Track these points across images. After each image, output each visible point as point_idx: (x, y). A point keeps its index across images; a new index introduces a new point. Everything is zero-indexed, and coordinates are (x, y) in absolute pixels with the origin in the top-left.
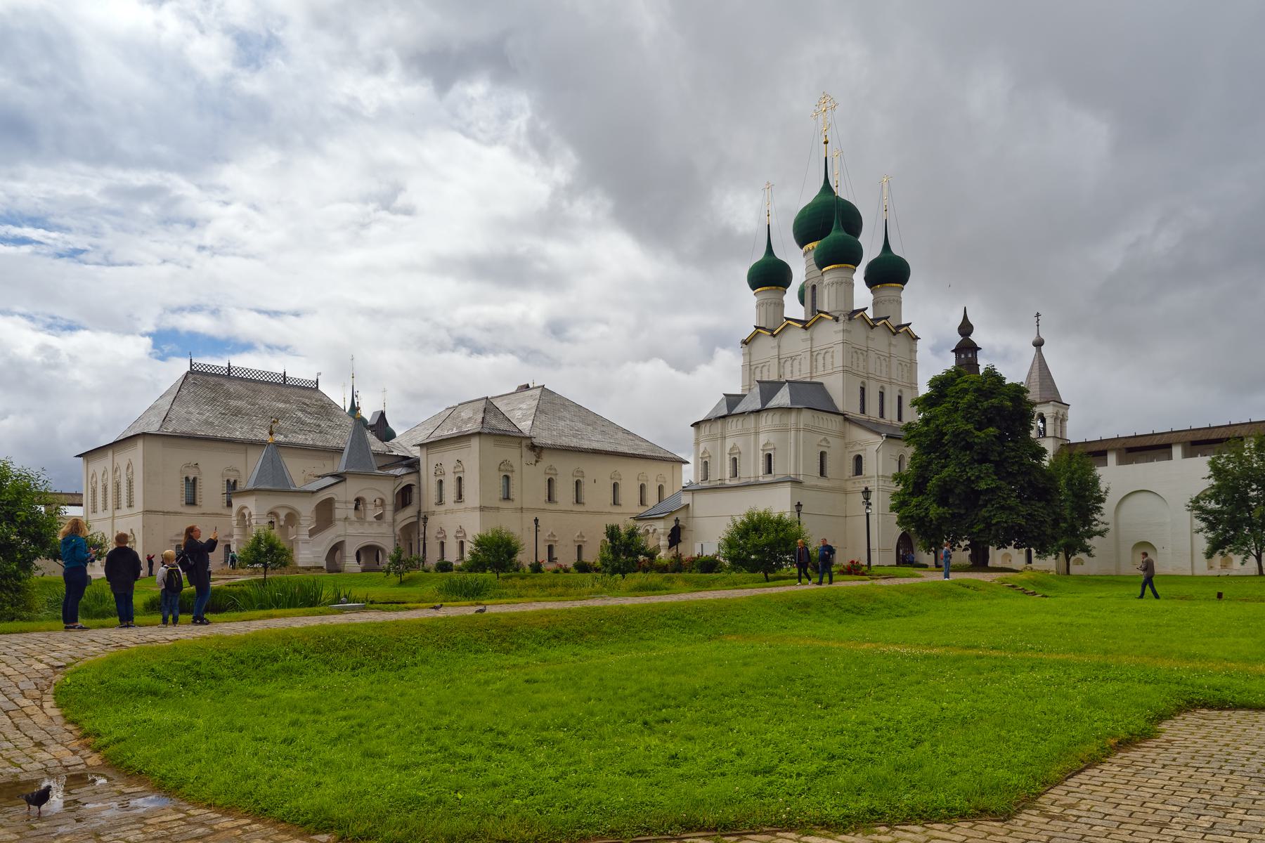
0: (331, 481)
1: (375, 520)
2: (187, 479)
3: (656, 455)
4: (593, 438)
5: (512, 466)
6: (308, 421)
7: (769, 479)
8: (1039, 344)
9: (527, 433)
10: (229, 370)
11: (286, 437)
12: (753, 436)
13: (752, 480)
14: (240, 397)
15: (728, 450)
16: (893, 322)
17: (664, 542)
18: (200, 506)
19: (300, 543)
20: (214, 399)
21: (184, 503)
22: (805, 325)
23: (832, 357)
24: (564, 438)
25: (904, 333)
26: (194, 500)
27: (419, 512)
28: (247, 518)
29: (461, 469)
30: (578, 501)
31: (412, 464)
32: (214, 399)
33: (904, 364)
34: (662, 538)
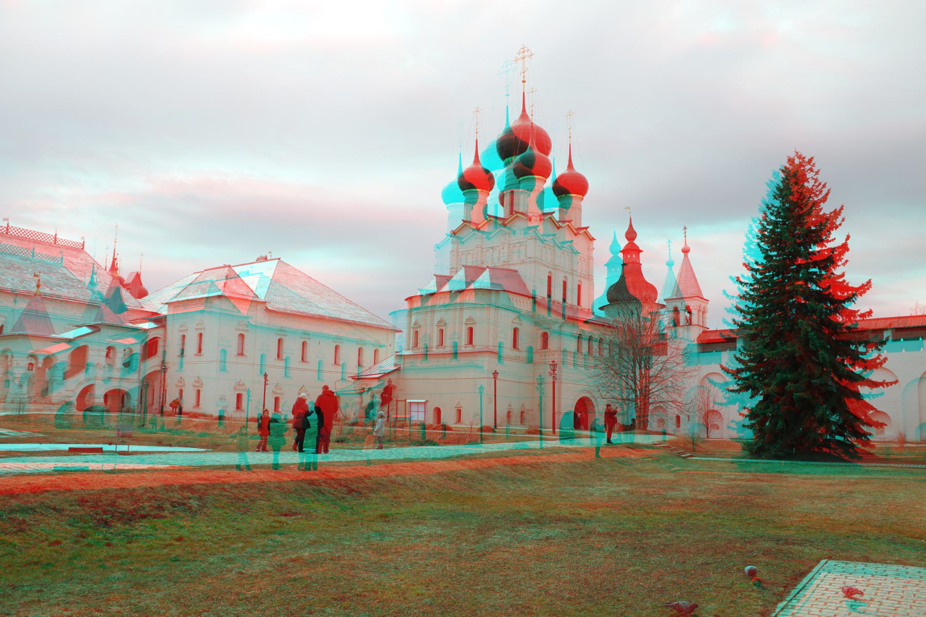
0: (86, 330)
1: (123, 366)
3: (374, 323)
4: (320, 306)
6: (72, 277)
7: (470, 349)
8: (686, 251)
9: (262, 297)
10: (7, 230)
11: (51, 289)
12: (458, 312)
15: (436, 322)
16: (575, 225)
17: (378, 399)
19: (55, 383)
22: (504, 222)
23: (526, 250)
24: (294, 304)
27: (163, 362)
28: (9, 359)
29: (203, 327)
31: (160, 321)
33: (583, 259)
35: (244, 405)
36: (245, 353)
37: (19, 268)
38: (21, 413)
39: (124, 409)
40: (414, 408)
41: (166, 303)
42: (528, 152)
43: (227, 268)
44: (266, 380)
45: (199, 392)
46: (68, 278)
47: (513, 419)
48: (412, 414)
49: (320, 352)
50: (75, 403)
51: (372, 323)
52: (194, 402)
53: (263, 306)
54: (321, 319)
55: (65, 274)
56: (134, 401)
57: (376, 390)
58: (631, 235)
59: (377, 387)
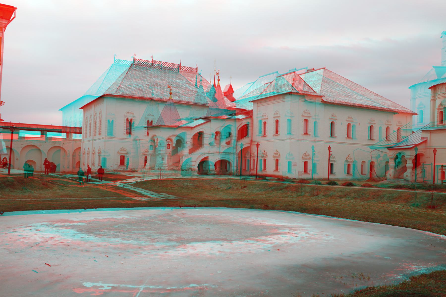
0: (201, 121)
1: (226, 145)
2: (127, 119)
3: (397, 109)
5: (309, 113)
9: (318, 93)
10: (152, 63)
11: (179, 97)
14: (157, 77)
18: (133, 135)
19: (184, 157)
20: (144, 77)
21: (125, 133)
26: (131, 131)
27: (251, 141)
28: (156, 142)
29: (278, 115)
30: (348, 137)
31: (248, 114)
32: (144, 77)
34: (408, 162)
36: (309, 133)
37: (160, 85)
38: (162, 178)
39: (228, 173)
41: (252, 101)
43: (293, 74)
45: (277, 161)
46: (189, 90)
50: (197, 169)
51: (395, 108)
52: (274, 167)
53: (320, 99)
55: (187, 87)
59: (410, 155)
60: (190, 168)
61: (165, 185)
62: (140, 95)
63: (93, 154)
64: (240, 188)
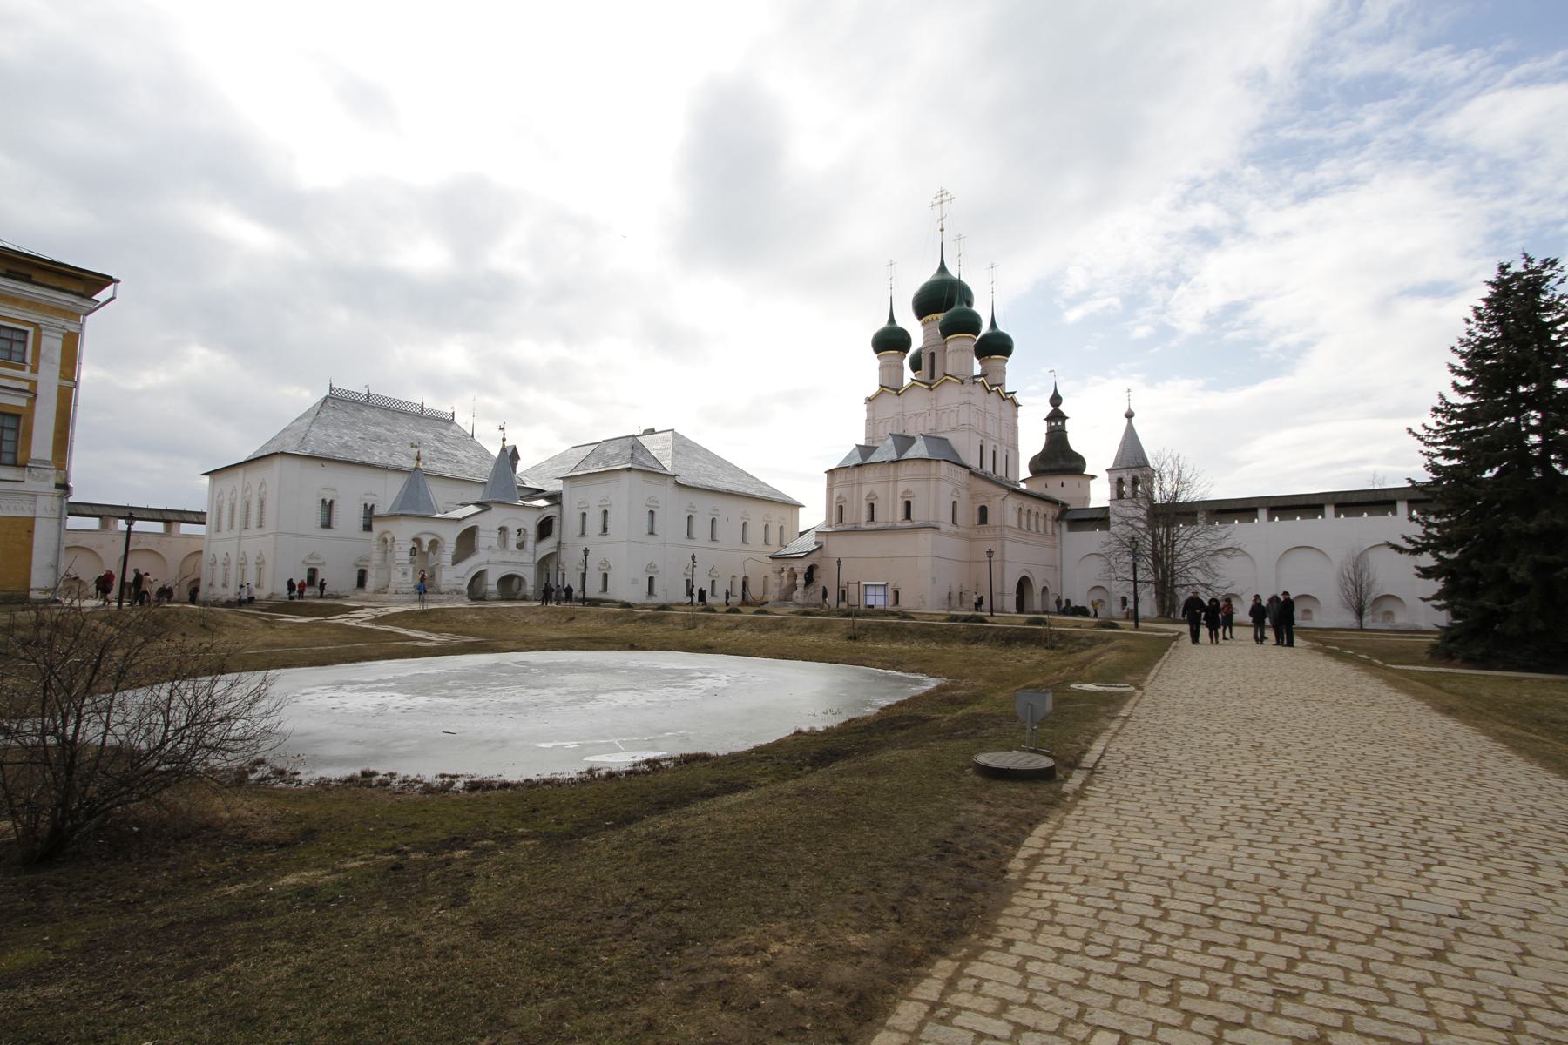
0: (473, 509)
2: (324, 501)
7: (908, 524)
8: (1130, 415)
9: (669, 470)
10: (368, 397)
11: (424, 464)
13: (890, 525)
14: (378, 424)
20: (353, 424)
21: (319, 525)
23: (957, 416)
25: (1010, 401)
27: (559, 543)
28: (389, 543)
30: (713, 538)
31: (555, 498)
32: (353, 424)
35: (657, 589)
36: (656, 531)
40: (870, 591)
42: (956, 308)
44: (694, 562)
47: (953, 601)
48: (869, 598)
49: (729, 532)
52: (600, 587)
54: (730, 494)
56: (530, 587)
57: (800, 570)
58: (1056, 400)
60: (455, 590)
61: (433, 619)
62: (350, 457)
63: (224, 565)
64: (564, 620)
